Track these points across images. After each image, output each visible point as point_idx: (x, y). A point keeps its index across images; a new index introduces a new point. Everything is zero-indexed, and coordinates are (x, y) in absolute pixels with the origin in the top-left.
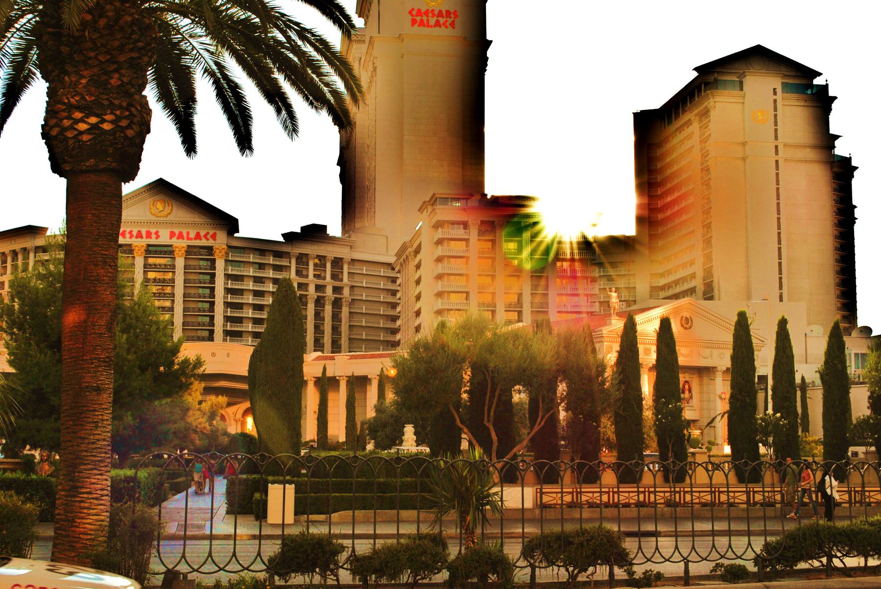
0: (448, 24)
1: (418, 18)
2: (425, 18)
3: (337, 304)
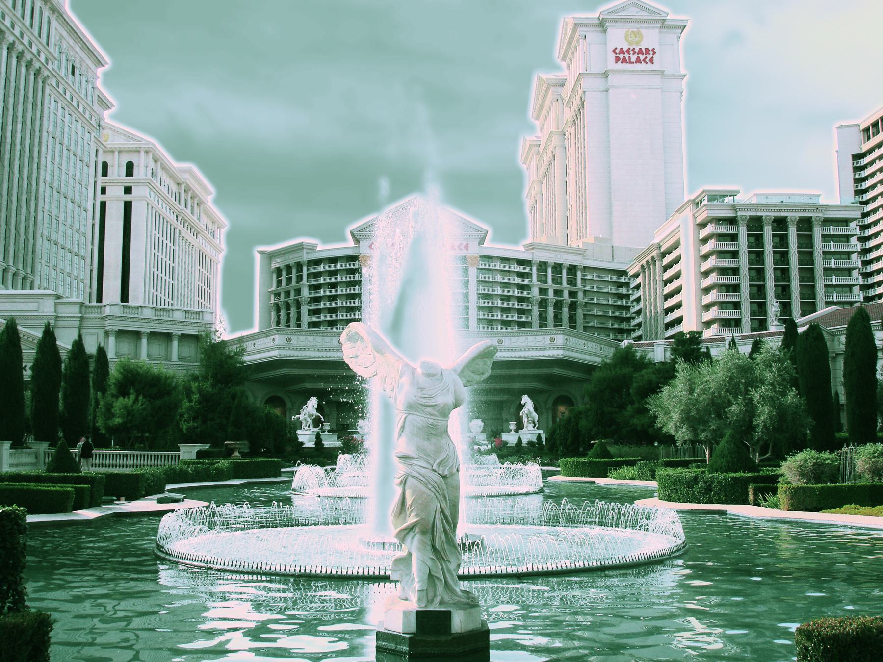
0: (647, 60)
1: (621, 56)
2: (627, 56)
3: (573, 306)
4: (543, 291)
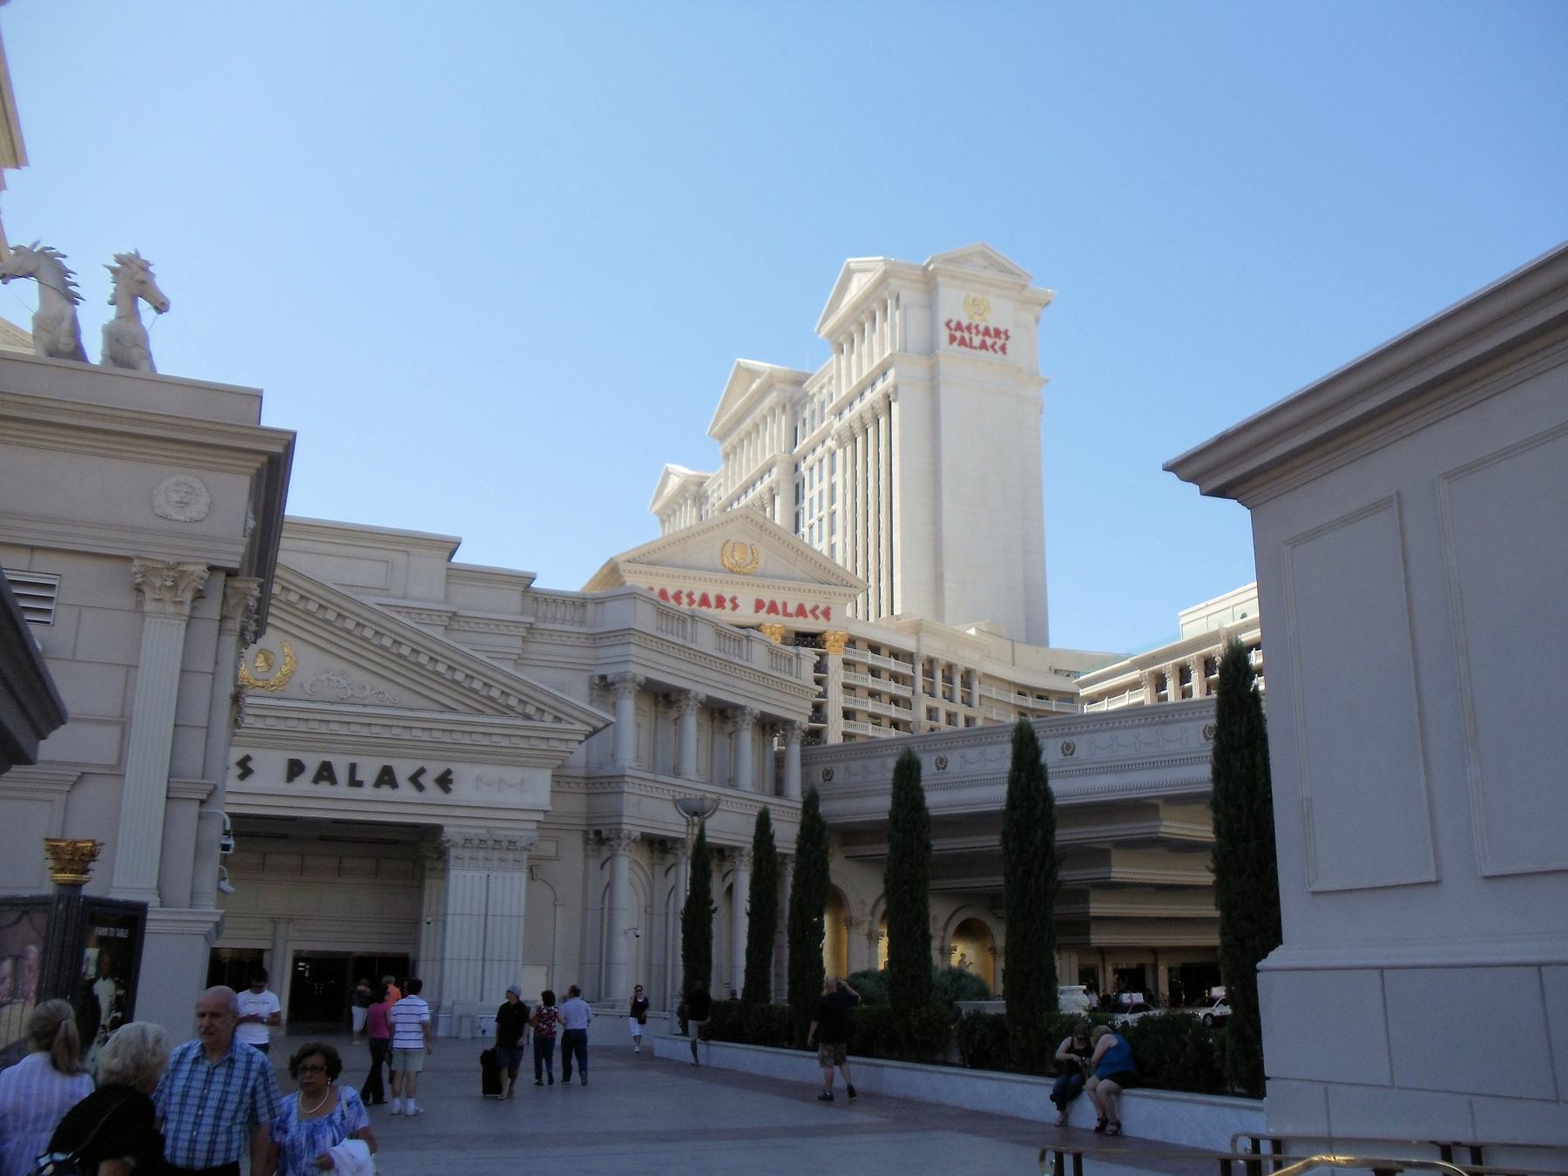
1: (958, 334)
2: (967, 335)
4: (932, 713)
